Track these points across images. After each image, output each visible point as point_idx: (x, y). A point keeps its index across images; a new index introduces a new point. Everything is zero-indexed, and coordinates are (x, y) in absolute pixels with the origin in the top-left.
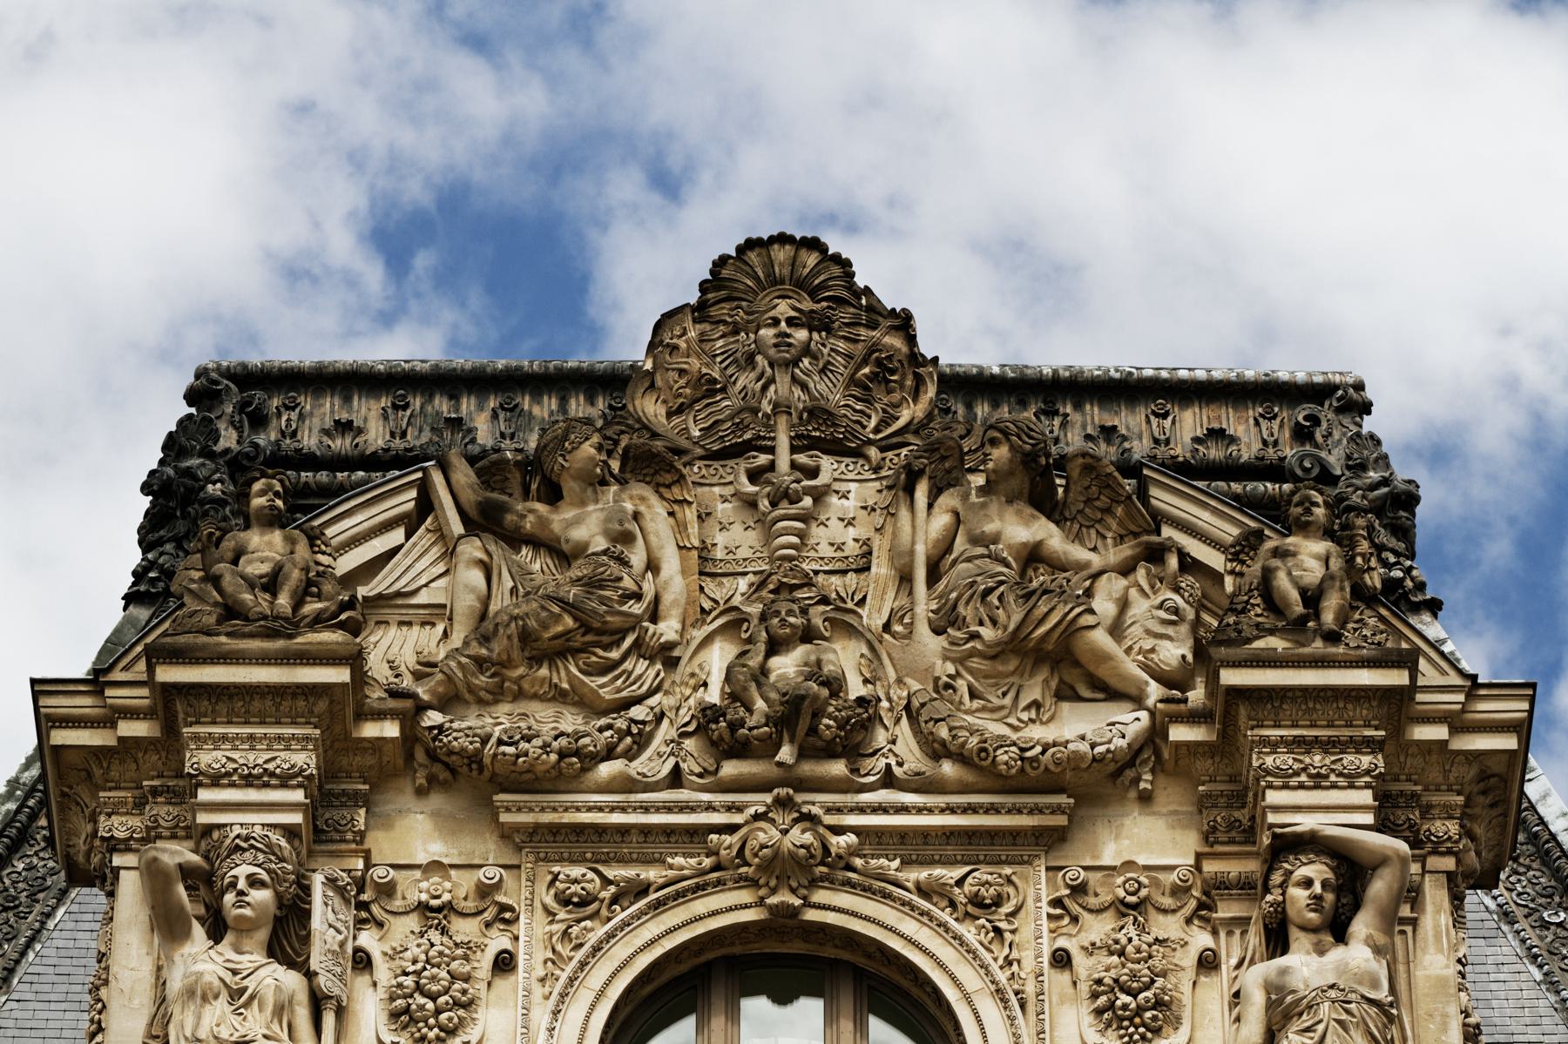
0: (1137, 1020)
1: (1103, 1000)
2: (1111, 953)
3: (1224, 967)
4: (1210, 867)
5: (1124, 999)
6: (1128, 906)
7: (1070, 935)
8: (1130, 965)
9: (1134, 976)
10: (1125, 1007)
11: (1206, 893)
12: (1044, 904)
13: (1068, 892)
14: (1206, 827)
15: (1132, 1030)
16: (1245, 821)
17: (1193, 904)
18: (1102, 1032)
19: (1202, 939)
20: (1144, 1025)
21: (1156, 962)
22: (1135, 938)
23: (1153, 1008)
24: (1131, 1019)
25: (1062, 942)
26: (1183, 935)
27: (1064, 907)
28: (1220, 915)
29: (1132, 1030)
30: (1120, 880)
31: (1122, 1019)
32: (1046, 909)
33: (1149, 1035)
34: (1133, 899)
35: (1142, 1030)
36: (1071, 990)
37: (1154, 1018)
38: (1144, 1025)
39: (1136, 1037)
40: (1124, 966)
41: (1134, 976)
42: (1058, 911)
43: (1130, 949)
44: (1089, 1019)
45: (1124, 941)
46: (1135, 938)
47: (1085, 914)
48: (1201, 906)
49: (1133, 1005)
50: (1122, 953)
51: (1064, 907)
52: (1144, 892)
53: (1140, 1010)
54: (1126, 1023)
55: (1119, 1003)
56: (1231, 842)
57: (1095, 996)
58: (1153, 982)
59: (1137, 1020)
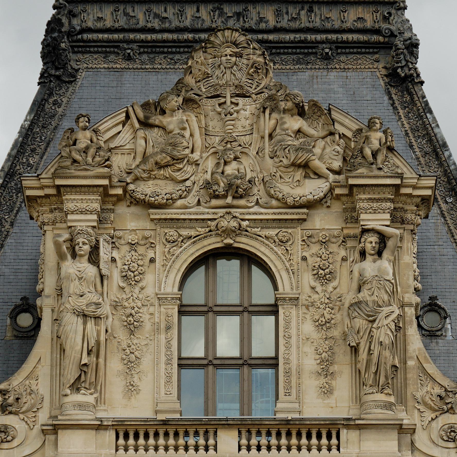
0: (324, 278)
1: (315, 272)
2: (318, 257)
3: (348, 261)
4: (346, 231)
5: (321, 272)
6: (323, 242)
7: (307, 251)
8: (323, 262)
9: (324, 265)
10: (321, 274)
11: (344, 238)
12: (300, 241)
13: (306, 238)
14: (345, 219)
15: (323, 281)
16: (355, 217)
17: (341, 241)
18: (315, 281)
19: (343, 253)
20: (326, 279)
21: (330, 260)
22: (325, 253)
23: (329, 274)
24: (323, 277)
25: (304, 254)
26: (338, 251)
27: (305, 242)
28: (348, 246)
29: (323, 281)
30: (321, 235)
31: (321, 277)
32: (300, 243)
33: (328, 282)
34: (324, 241)
35: (326, 281)
36: (306, 268)
37: (329, 277)
38: (326, 279)
39: (324, 283)
40: (321, 261)
41: (324, 265)
42: (304, 243)
43: (323, 257)
44: (311, 277)
45: (321, 254)
46: (325, 253)
47: (311, 244)
48: (343, 242)
49: (323, 274)
50: (321, 257)
51: (305, 242)
52: (327, 239)
53: (325, 275)
54: (321, 279)
55: (319, 273)
56: (352, 222)
57: (314, 270)
58: (329, 266)
59: (324, 278)
